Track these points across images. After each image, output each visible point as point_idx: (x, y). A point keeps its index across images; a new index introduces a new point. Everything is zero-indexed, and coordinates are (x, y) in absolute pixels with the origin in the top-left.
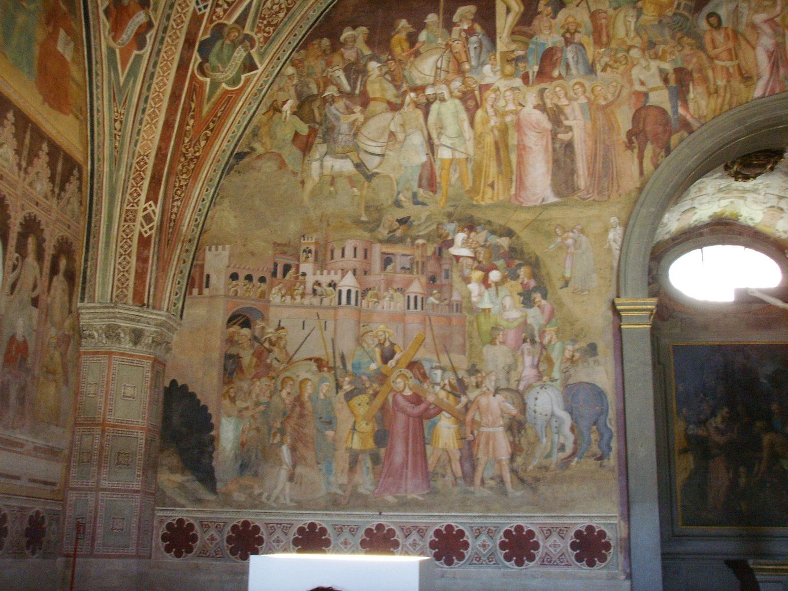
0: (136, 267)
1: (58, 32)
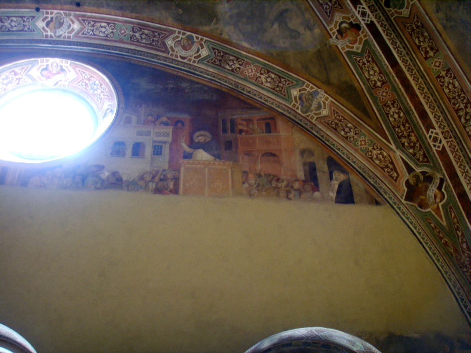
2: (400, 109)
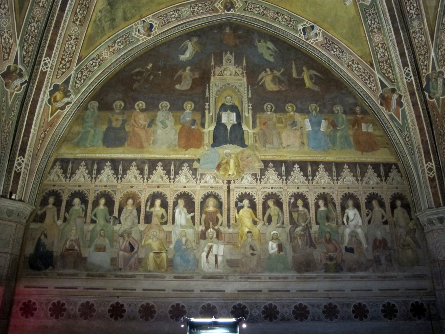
0: (432, 191)
1: (361, 127)
2: (38, 27)
